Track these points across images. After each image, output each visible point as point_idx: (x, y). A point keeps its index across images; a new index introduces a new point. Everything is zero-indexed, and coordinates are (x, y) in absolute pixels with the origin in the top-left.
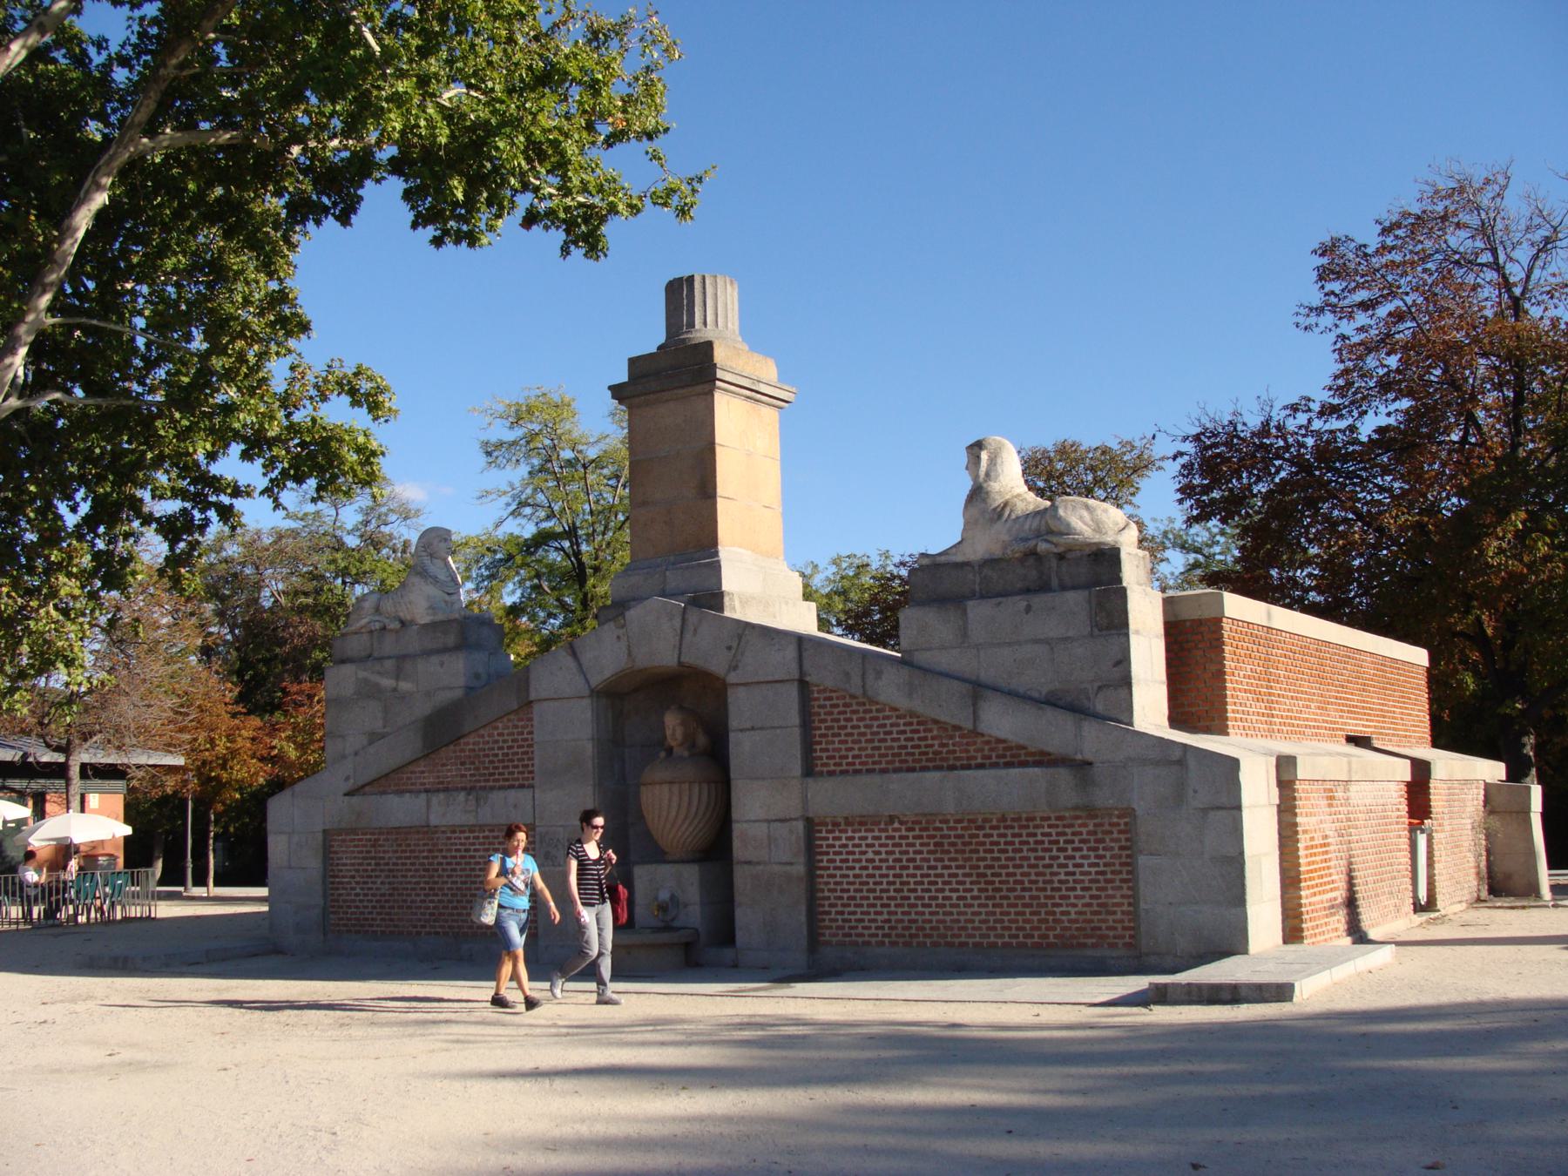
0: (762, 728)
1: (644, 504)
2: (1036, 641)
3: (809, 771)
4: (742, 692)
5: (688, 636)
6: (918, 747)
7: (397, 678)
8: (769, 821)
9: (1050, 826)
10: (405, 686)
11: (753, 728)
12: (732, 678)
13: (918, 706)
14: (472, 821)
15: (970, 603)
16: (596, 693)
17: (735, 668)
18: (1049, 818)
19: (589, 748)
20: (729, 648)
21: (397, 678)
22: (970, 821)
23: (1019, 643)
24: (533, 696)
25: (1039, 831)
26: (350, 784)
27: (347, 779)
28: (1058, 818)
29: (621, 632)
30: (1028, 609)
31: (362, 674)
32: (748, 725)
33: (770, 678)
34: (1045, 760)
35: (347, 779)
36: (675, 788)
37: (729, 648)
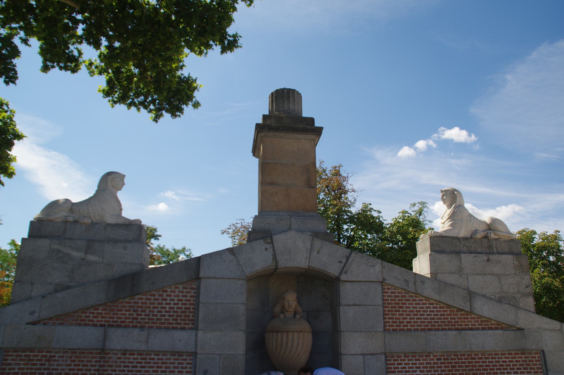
0: (360, 305)
1: (271, 184)
2: (493, 274)
3: (385, 330)
4: (348, 285)
5: (314, 254)
6: (441, 319)
7: (86, 253)
8: (364, 355)
9: (505, 358)
10: (92, 258)
11: (355, 305)
12: (343, 277)
13: (443, 299)
14: (143, 347)
15: (462, 255)
16: (249, 279)
17: (346, 272)
18: (505, 354)
19: (242, 309)
20: (341, 262)
21: (86, 253)
22: (468, 355)
23: (485, 274)
24: (200, 276)
25: (501, 360)
26: (35, 317)
27: (32, 313)
28: (509, 354)
29: (268, 246)
30: (488, 260)
31: (56, 247)
32: (352, 303)
33: (366, 280)
34: (501, 326)
35: (32, 313)
36: (301, 334)
37: (341, 262)
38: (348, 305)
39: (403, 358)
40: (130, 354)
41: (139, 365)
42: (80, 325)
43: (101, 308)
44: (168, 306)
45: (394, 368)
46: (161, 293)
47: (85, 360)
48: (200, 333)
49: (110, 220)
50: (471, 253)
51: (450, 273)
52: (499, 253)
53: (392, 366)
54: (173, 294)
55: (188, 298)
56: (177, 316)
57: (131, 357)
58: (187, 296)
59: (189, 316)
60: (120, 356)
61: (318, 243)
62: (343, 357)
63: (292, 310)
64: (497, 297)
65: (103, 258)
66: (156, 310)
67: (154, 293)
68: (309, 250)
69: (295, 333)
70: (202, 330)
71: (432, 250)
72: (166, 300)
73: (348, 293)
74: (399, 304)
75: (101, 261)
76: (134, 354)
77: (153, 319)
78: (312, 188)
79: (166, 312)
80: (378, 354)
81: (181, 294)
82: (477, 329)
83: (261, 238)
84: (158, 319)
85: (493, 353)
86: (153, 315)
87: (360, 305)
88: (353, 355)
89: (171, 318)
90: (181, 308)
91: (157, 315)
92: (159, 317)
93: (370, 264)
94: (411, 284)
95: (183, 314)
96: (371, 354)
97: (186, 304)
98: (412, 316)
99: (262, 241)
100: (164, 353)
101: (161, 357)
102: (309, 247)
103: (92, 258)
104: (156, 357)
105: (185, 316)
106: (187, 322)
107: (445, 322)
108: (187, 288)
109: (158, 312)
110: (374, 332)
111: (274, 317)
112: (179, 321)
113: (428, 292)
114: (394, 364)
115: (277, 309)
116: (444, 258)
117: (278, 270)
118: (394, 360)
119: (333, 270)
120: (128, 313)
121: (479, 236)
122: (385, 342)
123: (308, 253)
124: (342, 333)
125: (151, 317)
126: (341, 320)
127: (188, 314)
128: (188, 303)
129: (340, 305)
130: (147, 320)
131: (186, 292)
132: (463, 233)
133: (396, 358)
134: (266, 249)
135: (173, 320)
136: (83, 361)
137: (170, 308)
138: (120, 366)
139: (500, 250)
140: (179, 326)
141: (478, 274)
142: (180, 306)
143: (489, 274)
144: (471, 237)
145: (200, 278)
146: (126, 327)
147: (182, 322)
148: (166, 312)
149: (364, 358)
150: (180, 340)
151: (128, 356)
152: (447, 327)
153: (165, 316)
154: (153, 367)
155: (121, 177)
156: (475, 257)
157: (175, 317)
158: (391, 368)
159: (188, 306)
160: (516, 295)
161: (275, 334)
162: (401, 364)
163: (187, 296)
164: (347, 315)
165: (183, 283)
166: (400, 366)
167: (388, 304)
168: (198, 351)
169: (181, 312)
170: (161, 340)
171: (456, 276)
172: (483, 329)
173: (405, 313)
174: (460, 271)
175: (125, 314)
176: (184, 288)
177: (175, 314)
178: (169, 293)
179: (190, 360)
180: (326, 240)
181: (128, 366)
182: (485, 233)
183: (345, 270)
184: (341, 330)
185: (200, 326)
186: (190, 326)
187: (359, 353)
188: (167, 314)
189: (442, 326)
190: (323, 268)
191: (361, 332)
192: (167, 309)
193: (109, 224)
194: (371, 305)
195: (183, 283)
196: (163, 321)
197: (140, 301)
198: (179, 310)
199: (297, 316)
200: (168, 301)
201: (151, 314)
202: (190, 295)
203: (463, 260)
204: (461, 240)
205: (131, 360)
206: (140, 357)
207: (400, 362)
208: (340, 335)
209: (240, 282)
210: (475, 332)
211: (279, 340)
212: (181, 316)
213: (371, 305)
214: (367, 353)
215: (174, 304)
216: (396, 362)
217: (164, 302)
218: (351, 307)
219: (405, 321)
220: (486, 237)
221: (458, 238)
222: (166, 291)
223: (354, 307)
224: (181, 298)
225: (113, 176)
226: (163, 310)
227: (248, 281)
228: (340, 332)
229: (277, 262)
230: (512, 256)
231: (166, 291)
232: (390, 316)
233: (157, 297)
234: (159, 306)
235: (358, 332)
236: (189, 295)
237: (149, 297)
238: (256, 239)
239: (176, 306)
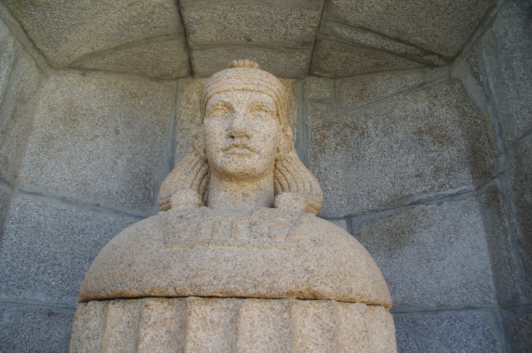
69: (252, 311)
199: (284, 199)
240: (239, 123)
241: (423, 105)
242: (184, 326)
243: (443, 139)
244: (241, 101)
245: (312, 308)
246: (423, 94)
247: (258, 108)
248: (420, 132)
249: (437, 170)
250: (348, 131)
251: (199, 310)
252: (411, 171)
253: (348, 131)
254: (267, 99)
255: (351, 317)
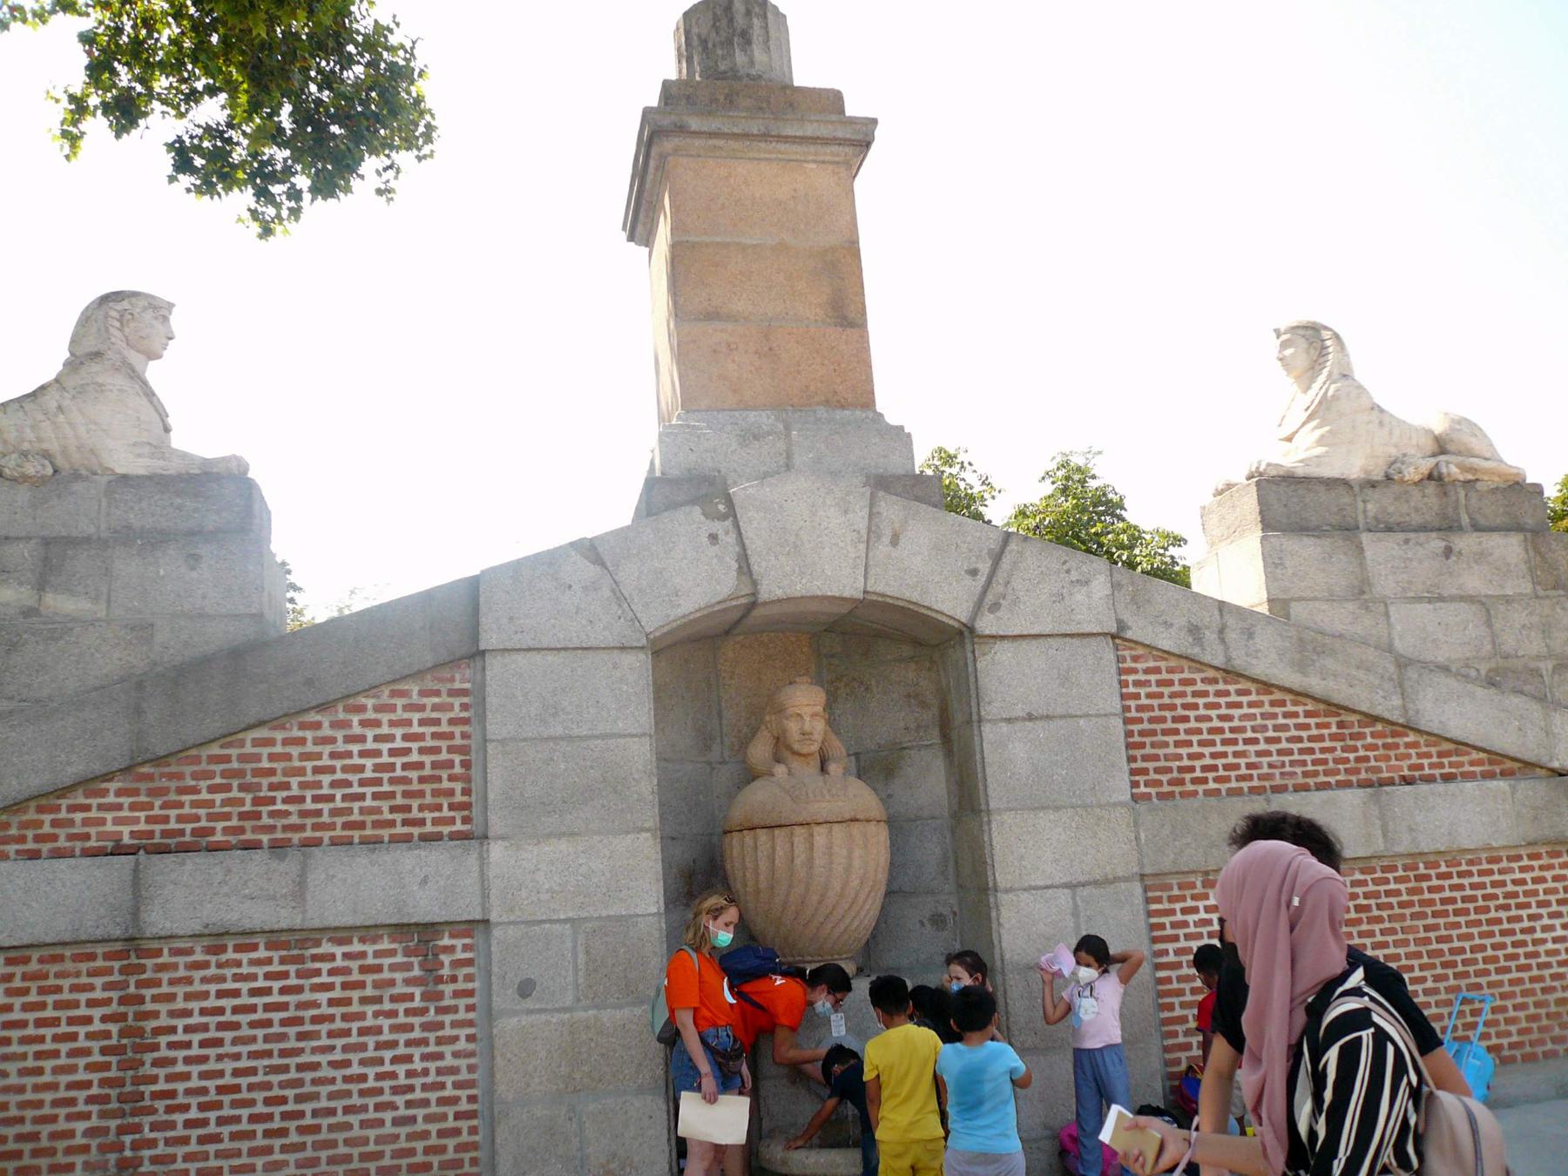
0: (1048, 717)
1: (712, 316)
9: (1522, 869)
11: (1030, 717)
13: (1315, 684)
14: (285, 917)
17: (995, 607)
19: (641, 754)
20: (974, 573)
21: (41, 586)
23: (1441, 599)
24: (482, 647)
28: (1531, 857)
29: (718, 527)
30: (1448, 552)
32: (1019, 711)
36: (856, 829)
38: (1009, 720)
39: (1199, 889)
40: (238, 948)
41: (276, 985)
42: (34, 855)
43: (113, 786)
44: (369, 763)
45: (1174, 925)
46: (341, 716)
47: (66, 983)
48: (496, 850)
49: (125, 460)
50: (1389, 529)
51: (1331, 599)
52: (1476, 528)
53: (1166, 920)
54: (385, 718)
55: (444, 728)
56: (406, 794)
57: (245, 957)
58: (437, 722)
59: (451, 793)
60: (199, 956)
61: (892, 509)
62: (1004, 898)
63: (815, 747)
64: (1483, 673)
65: (109, 601)
66: (326, 779)
67: (313, 717)
68: (864, 532)
70: (503, 838)
71: (1267, 524)
72: (362, 739)
73: (1006, 679)
74: (1173, 707)
75: (102, 614)
76: (254, 947)
77: (319, 813)
78: (852, 325)
79: (362, 783)
80: (1116, 879)
81: (416, 717)
82: (1430, 779)
83: (693, 502)
84: (335, 812)
85: (1484, 856)
86: (316, 799)
87: (1048, 717)
88: (1036, 888)
89: (385, 805)
90: (419, 766)
91: (331, 798)
92: (339, 803)
93: (1074, 576)
94: (1210, 636)
95: (428, 788)
96: (1096, 883)
97: (437, 750)
98: (1219, 748)
99: (697, 510)
100: (368, 932)
101: (356, 947)
102: (862, 525)
103: (59, 603)
104: (339, 951)
105: (435, 793)
106: (446, 813)
107: (1325, 762)
108: (437, 693)
109: (334, 784)
110: (1101, 806)
111: (751, 776)
112: (415, 814)
113: (1268, 660)
114: (1172, 912)
115: (760, 751)
116: (1306, 550)
117: (756, 613)
118: (1171, 899)
119: (949, 599)
120: (218, 797)
121: (1411, 474)
122: (1137, 838)
123: (862, 547)
124: (996, 818)
125: (309, 805)
126: (989, 771)
127: (446, 784)
128: (444, 744)
129: (980, 721)
130: (294, 820)
131: (435, 708)
132: (1353, 464)
133: (1176, 892)
134: (713, 538)
135: (393, 809)
136: (58, 989)
137: (378, 768)
138: (205, 995)
139: (1482, 522)
140: (416, 831)
141: (1418, 599)
142: (415, 757)
143: (1452, 599)
144: (1388, 478)
145: (483, 653)
146: (214, 848)
147: (429, 816)
148: (362, 783)
149: (1074, 898)
150: (425, 881)
151: (230, 955)
152: (1332, 780)
153: (362, 797)
154: (329, 987)
155: (160, 309)
156: (1407, 541)
157: (399, 801)
158: (1162, 926)
159: (444, 756)
160: (1542, 665)
161: (763, 835)
162: (1195, 910)
163: (437, 722)
164: (1007, 753)
165: (418, 675)
166: (1191, 918)
167: (1140, 708)
168: (493, 917)
169: (422, 780)
170: (355, 886)
171: (1350, 606)
172: (1448, 778)
173: (1195, 738)
174: (1361, 591)
175: (211, 804)
176: (423, 693)
177: (399, 789)
178: (370, 715)
179: (466, 948)
180: (917, 499)
181: (235, 993)
182: (1433, 461)
183: (990, 598)
184: (992, 805)
185: (497, 824)
186: (459, 826)
187: (1057, 881)
188: (369, 790)
189: (1315, 774)
190: (915, 597)
191: (1057, 809)
192: (368, 774)
193: (125, 478)
194: (1087, 716)
195: (418, 675)
196: (356, 817)
197: (265, 751)
198: (414, 775)
200: (370, 745)
201: (309, 794)
202: (452, 715)
203: (1368, 554)
204: (1357, 489)
205: (245, 970)
206: (276, 955)
207: (1190, 903)
208: (989, 822)
209: (628, 659)
210: (1424, 788)
211: (780, 852)
212: (421, 794)
213: (1087, 716)
214: (1082, 879)
215: (392, 753)
216: (1178, 906)
217: (355, 748)
218: (1018, 726)
219: (1198, 764)
220: (1433, 477)
221: (1345, 483)
222: (361, 709)
223: (1029, 724)
224: (416, 729)
225: (125, 304)
226: (354, 778)
227: (656, 654)
228: (988, 812)
229: (755, 583)
230: (1521, 536)
231: (361, 709)
232: (1148, 750)
233: (327, 731)
234: (338, 764)
235: (1048, 807)
236: (445, 717)
237: (297, 733)
238: (673, 506)
239: (399, 761)
240: (807, 727)
241: (911, 675)
242: (812, 835)
243: (924, 705)
244: (806, 711)
245: (857, 824)
246: (913, 666)
247: (814, 715)
248: (909, 696)
249: (919, 727)
250: (856, 684)
251: (817, 829)
252: (902, 724)
253: (856, 684)
254: (819, 709)
255: (872, 827)
